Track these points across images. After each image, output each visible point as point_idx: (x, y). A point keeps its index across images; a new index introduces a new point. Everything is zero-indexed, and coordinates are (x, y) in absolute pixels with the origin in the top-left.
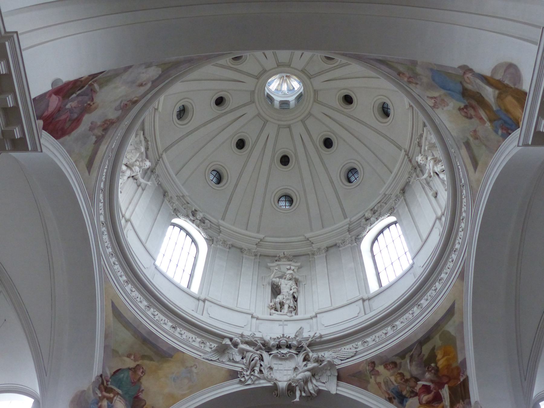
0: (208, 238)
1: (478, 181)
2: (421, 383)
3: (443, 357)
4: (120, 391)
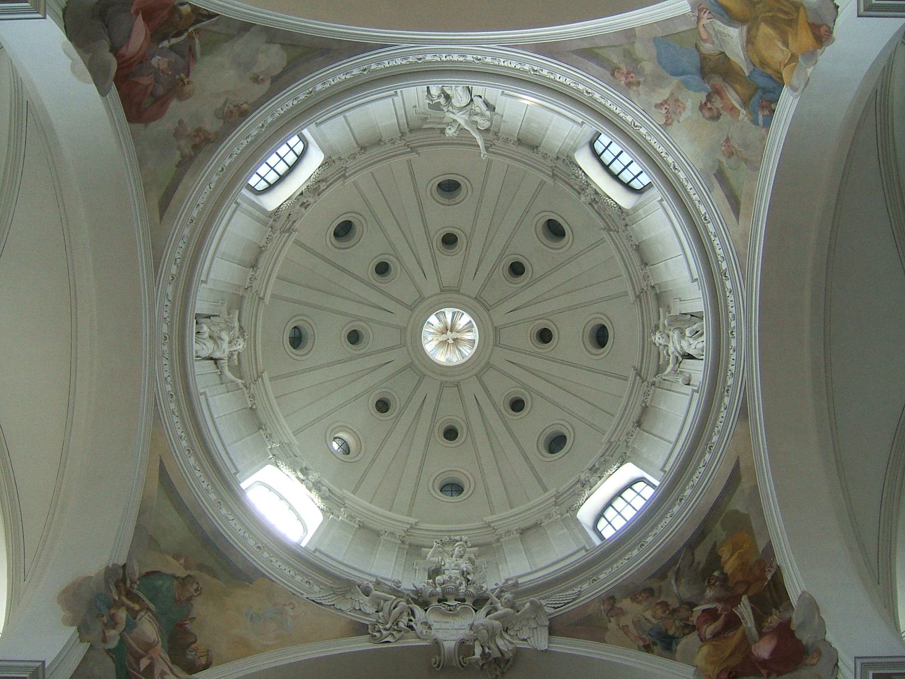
2: (698, 609)
4: (152, 606)
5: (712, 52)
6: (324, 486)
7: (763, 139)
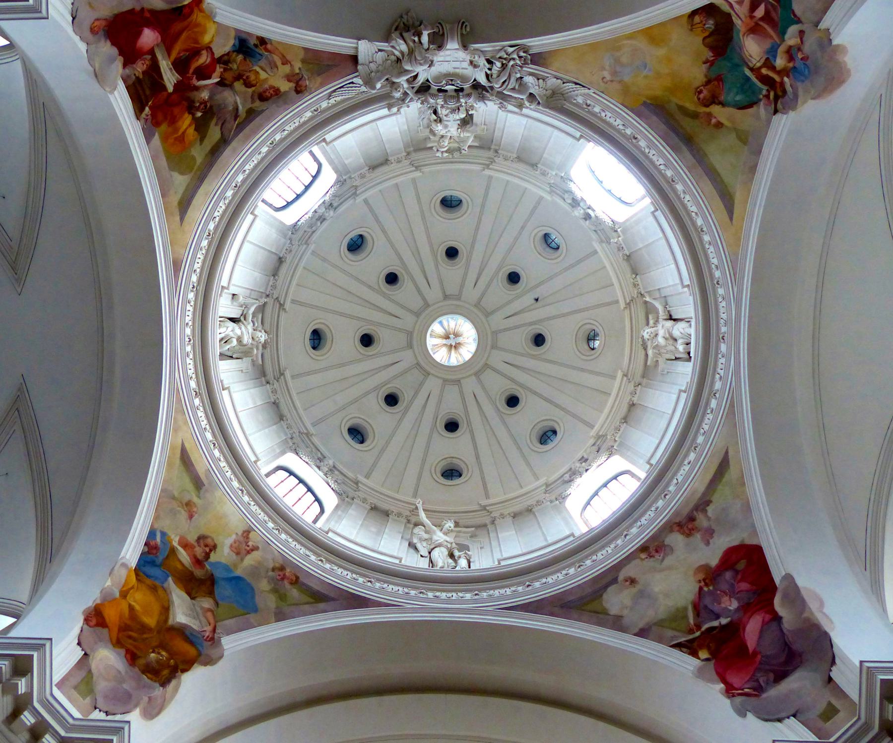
0: (569, 183)
1: (176, 430)
2: (215, 80)
5: (202, 599)
6: (570, 204)
7: (157, 518)
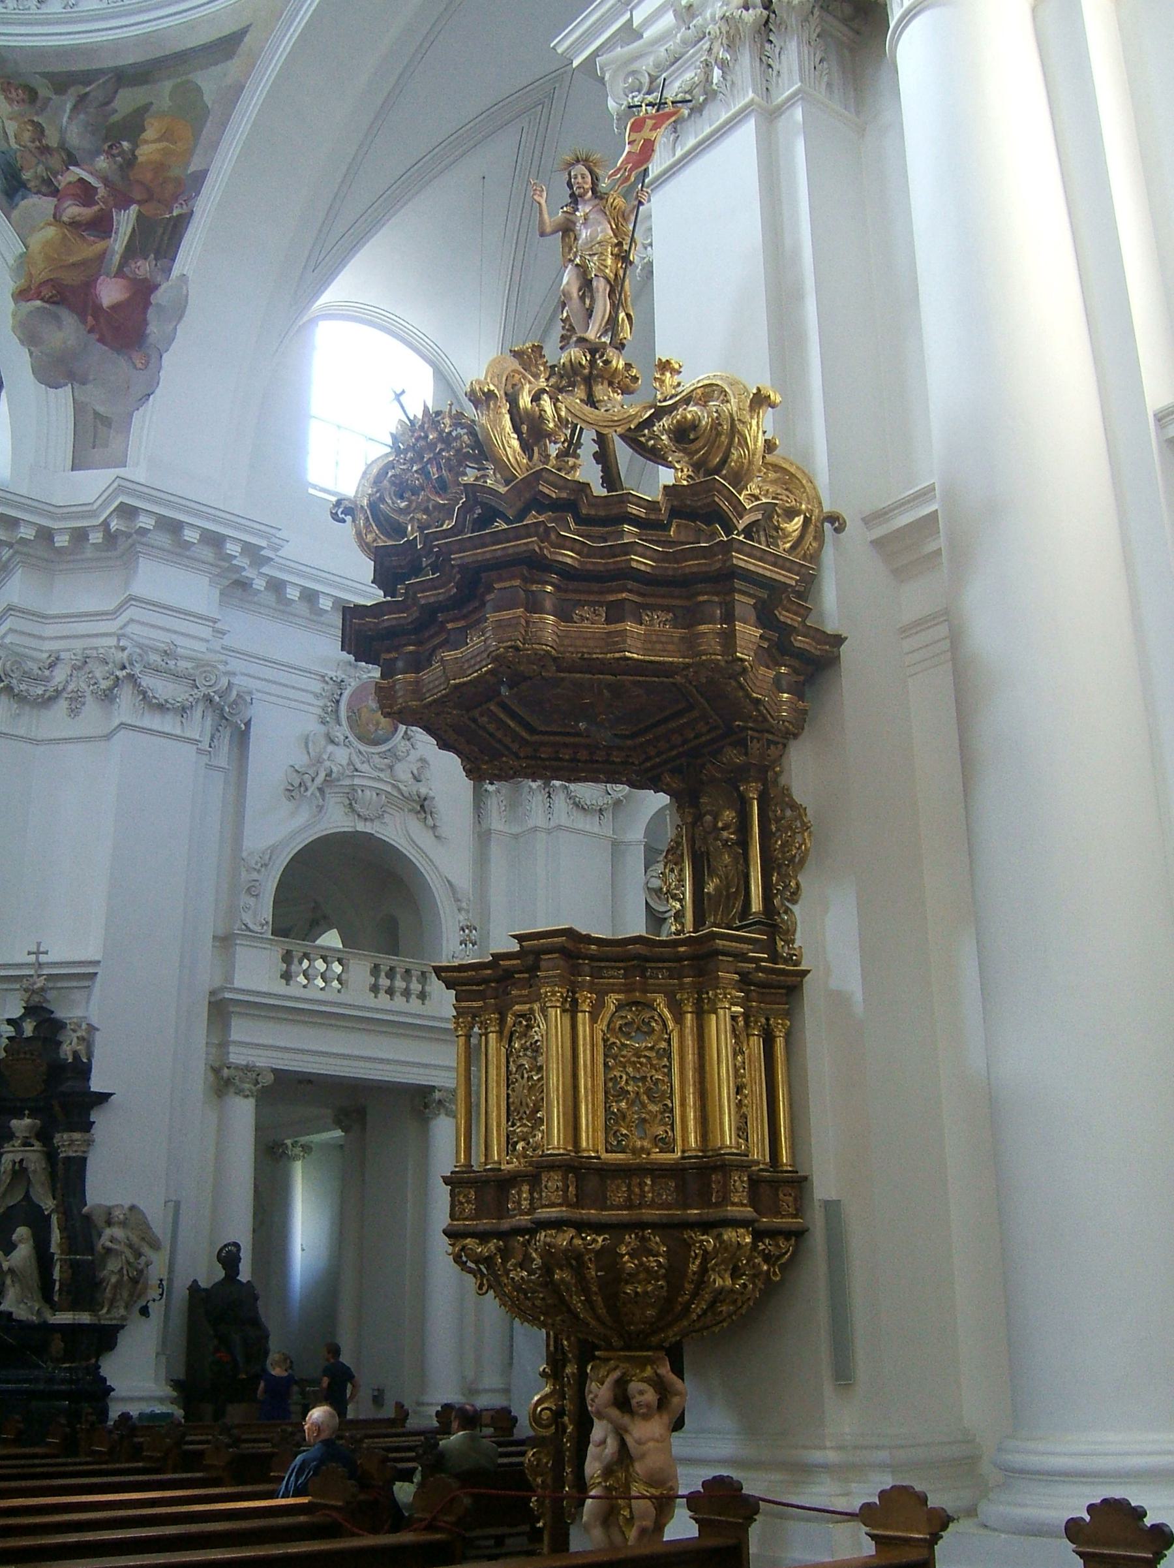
2: (77, 172)
3: (159, 140)
